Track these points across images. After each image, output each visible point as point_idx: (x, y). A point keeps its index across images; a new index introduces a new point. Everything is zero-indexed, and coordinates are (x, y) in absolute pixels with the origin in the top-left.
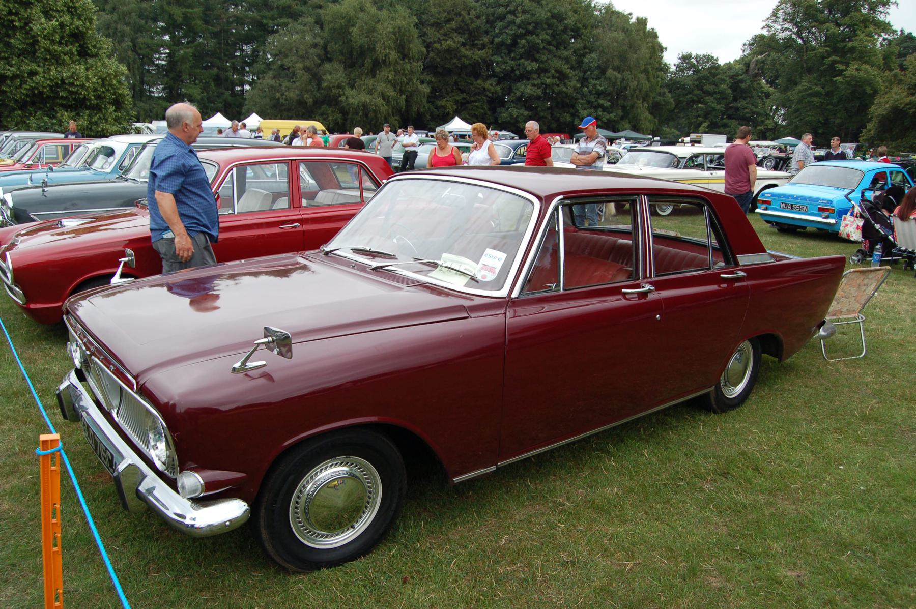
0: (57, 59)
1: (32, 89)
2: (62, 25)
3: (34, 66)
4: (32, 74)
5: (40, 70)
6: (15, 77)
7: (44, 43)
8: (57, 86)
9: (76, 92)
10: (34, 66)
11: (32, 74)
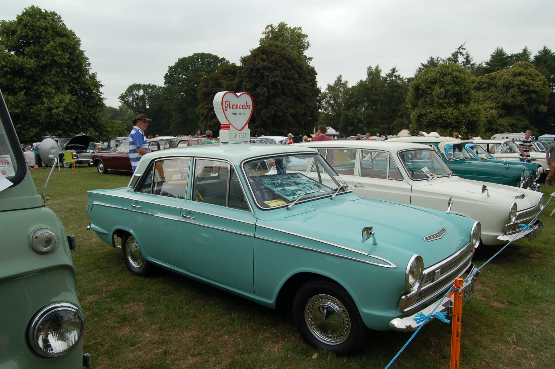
0: (441, 106)
1: (429, 119)
2: (447, 91)
3: (431, 110)
4: (431, 112)
5: (433, 111)
6: (426, 114)
7: (436, 99)
8: (439, 118)
9: (446, 120)
10: (431, 110)
11: (431, 112)
